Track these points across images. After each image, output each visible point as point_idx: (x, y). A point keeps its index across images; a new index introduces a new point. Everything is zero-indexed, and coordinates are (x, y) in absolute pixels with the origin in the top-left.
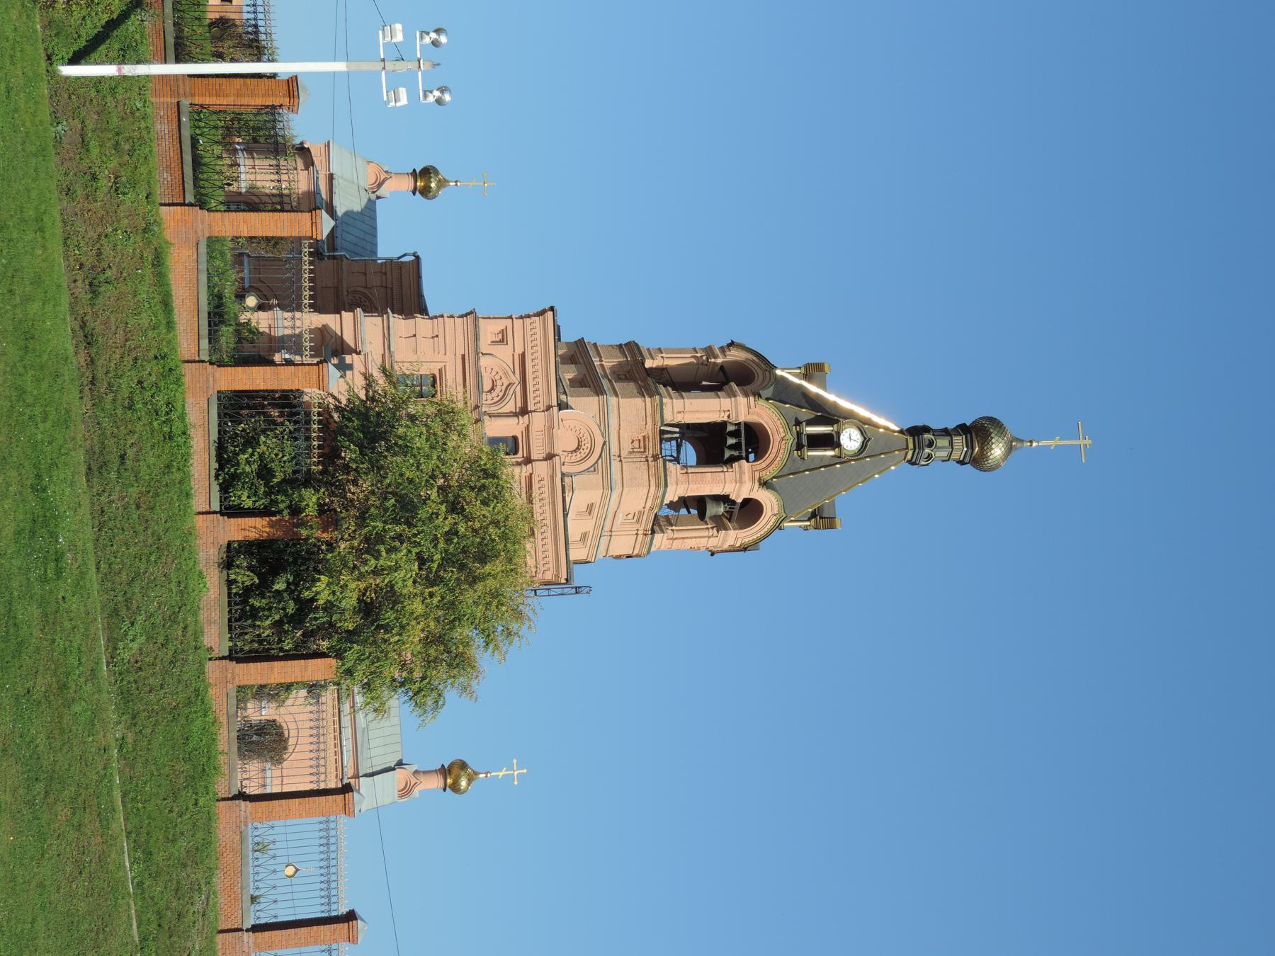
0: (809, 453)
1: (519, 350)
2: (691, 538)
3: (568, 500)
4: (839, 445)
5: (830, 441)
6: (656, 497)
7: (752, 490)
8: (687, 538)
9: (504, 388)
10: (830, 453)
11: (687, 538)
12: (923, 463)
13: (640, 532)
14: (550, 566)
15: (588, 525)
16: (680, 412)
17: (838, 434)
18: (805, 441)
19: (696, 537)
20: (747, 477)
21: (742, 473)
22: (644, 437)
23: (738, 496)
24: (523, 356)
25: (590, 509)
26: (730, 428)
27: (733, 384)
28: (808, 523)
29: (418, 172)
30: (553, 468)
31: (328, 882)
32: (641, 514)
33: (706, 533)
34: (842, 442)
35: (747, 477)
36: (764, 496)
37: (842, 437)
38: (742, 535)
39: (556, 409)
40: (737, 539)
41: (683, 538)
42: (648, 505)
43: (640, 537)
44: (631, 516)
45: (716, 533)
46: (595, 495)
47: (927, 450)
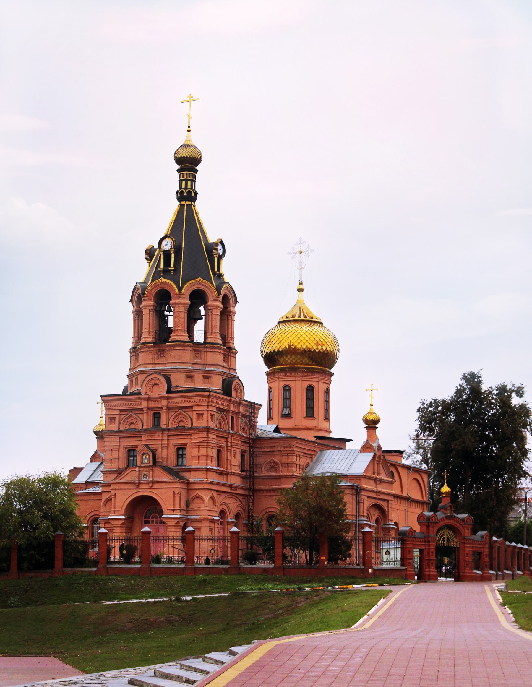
0: (172, 265)
1: (117, 412)
2: (212, 323)
3: (181, 389)
4: (169, 251)
5: (167, 254)
6: (184, 346)
7: (184, 298)
8: (212, 325)
9: (134, 419)
10: (173, 255)
11: (212, 325)
12: (193, 195)
13: (205, 350)
14: (204, 399)
15: (198, 377)
16: (149, 335)
17: (165, 251)
18: (166, 268)
19: (212, 320)
20: (177, 301)
21: (175, 303)
22: (159, 351)
23: (187, 304)
24: (120, 410)
25: (189, 377)
26: (158, 309)
27: (141, 306)
28: (216, 259)
29: (96, 436)
30: (164, 398)
31: (140, 540)
32: (195, 351)
33: (210, 315)
34: (168, 249)
35: (177, 301)
36: (187, 289)
37: (166, 249)
38: (211, 297)
39: (140, 396)
40: (214, 300)
41: (212, 327)
42: (189, 348)
43: (208, 350)
44: (197, 355)
45: (211, 311)
46: (183, 376)
47: (185, 194)
